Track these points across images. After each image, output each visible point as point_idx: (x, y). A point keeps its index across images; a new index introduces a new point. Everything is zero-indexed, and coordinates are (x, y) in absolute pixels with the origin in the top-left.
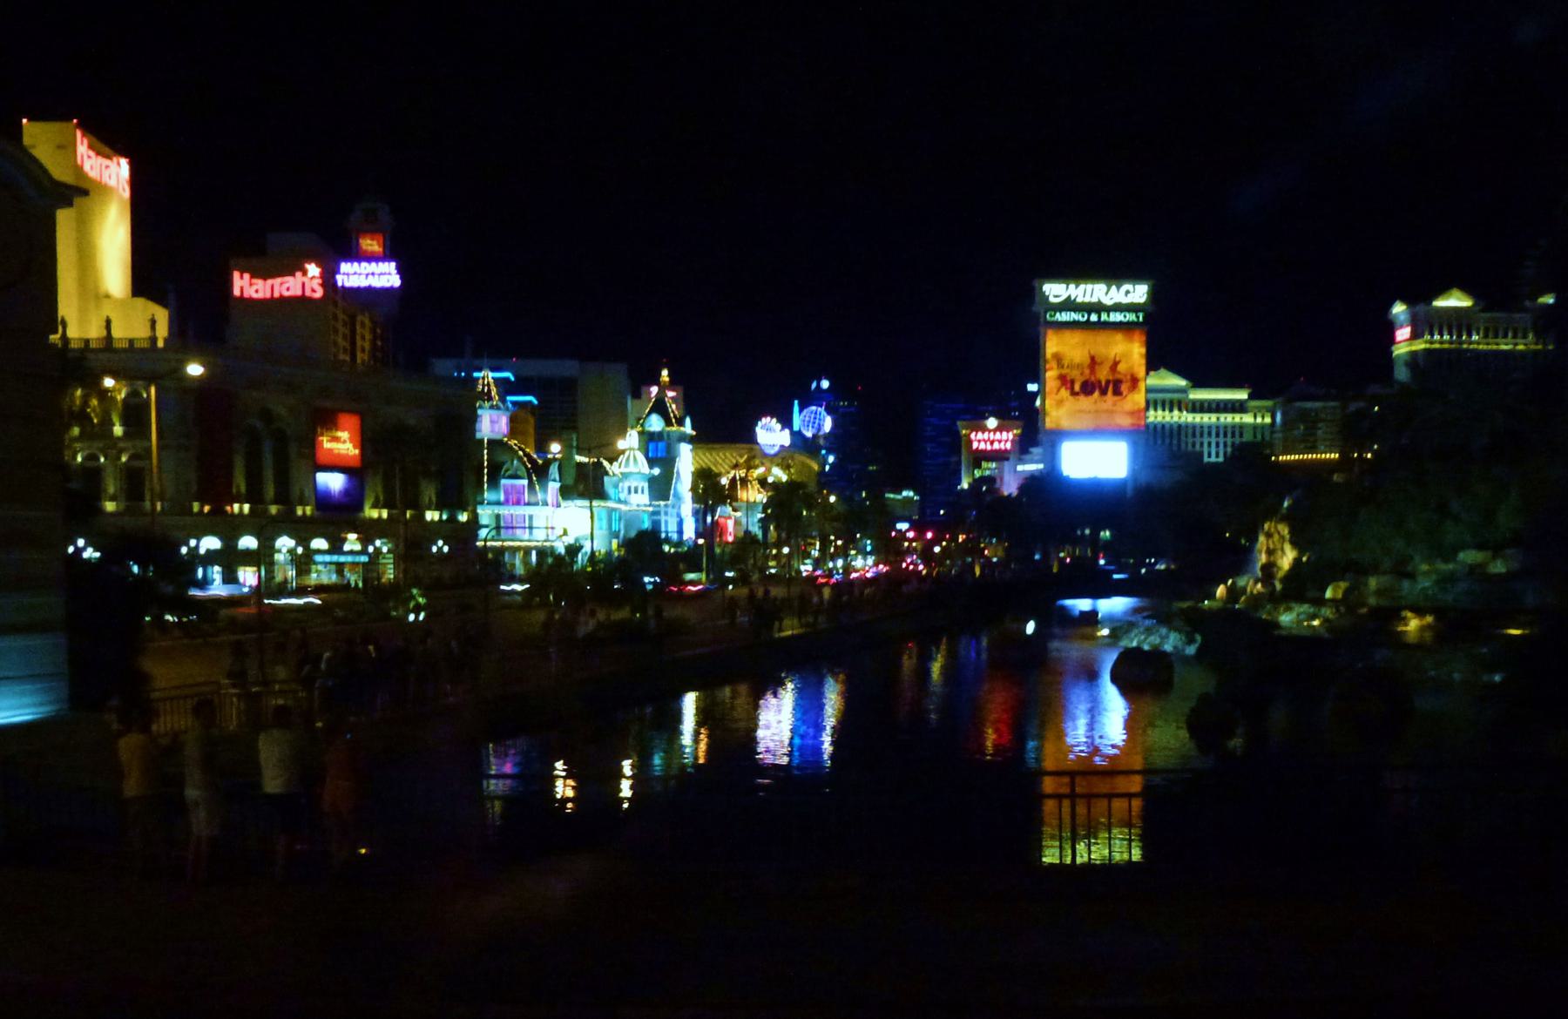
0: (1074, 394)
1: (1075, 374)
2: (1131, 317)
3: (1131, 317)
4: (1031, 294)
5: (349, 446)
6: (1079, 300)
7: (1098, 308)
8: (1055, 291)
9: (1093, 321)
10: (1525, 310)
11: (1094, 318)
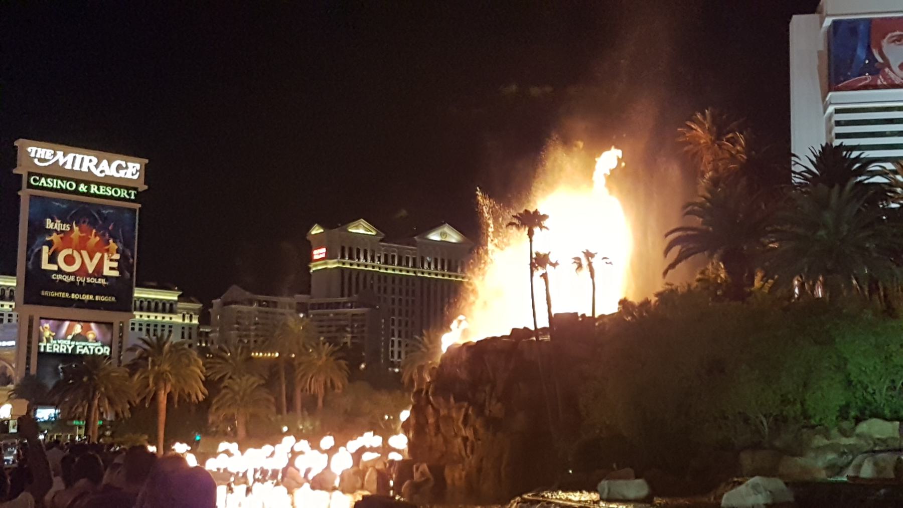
4: (12, 156)
10: (414, 244)
11: (83, 188)
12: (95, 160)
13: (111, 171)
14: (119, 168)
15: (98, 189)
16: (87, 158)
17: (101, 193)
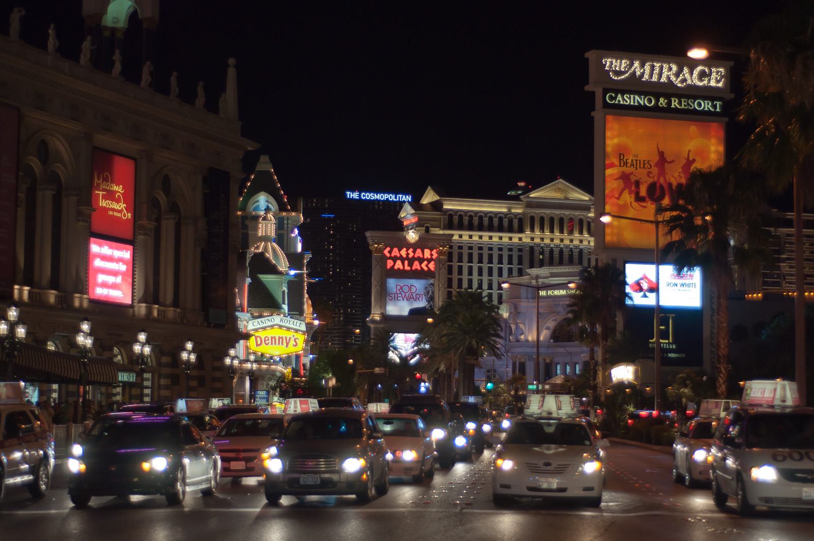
0: (639, 199)
1: (640, 174)
2: (706, 105)
3: (706, 105)
4: (582, 71)
5: (122, 206)
8: (616, 65)
9: (666, 105)
11: (662, 102)
12: (674, 68)
15: (680, 103)
17: (683, 107)
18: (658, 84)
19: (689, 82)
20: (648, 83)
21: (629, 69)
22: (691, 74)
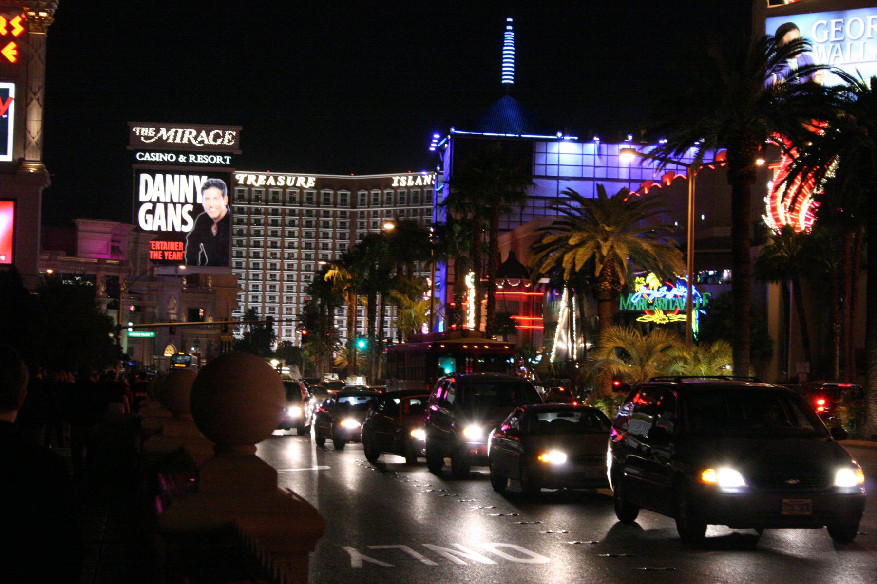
6: (171, 140)
7: (188, 149)
8: (145, 132)
11: (182, 158)
12: (194, 133)
13: (210, 140)
14: (217, 137)
15: (196, 159)
16: (187, 131)
18: (181, 144)
19: (206, 142)
20: (174, 144)
21: (156, 135)
22: (208, 135)
